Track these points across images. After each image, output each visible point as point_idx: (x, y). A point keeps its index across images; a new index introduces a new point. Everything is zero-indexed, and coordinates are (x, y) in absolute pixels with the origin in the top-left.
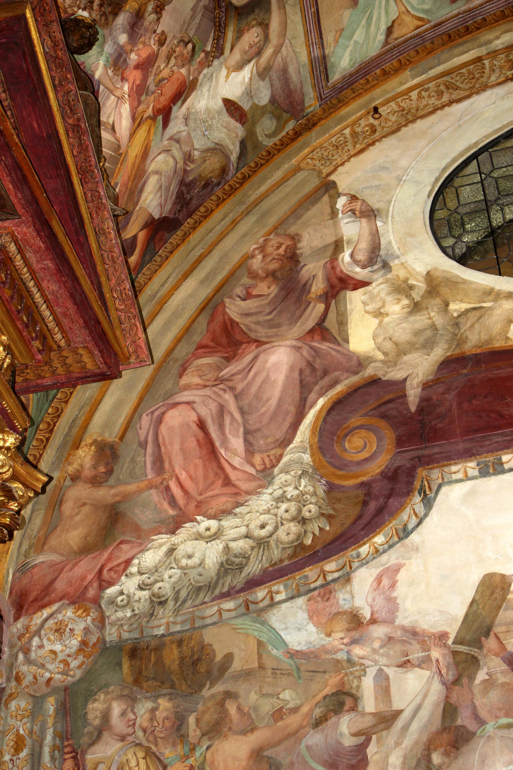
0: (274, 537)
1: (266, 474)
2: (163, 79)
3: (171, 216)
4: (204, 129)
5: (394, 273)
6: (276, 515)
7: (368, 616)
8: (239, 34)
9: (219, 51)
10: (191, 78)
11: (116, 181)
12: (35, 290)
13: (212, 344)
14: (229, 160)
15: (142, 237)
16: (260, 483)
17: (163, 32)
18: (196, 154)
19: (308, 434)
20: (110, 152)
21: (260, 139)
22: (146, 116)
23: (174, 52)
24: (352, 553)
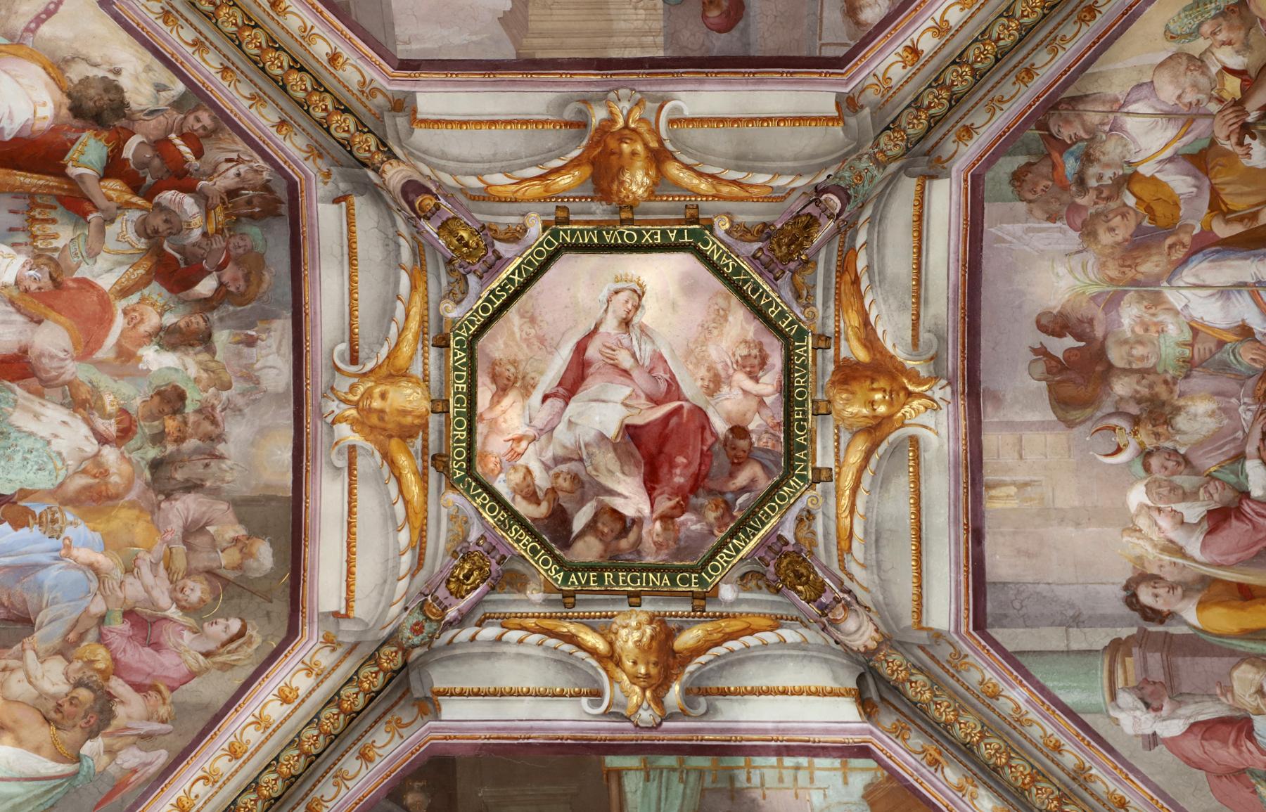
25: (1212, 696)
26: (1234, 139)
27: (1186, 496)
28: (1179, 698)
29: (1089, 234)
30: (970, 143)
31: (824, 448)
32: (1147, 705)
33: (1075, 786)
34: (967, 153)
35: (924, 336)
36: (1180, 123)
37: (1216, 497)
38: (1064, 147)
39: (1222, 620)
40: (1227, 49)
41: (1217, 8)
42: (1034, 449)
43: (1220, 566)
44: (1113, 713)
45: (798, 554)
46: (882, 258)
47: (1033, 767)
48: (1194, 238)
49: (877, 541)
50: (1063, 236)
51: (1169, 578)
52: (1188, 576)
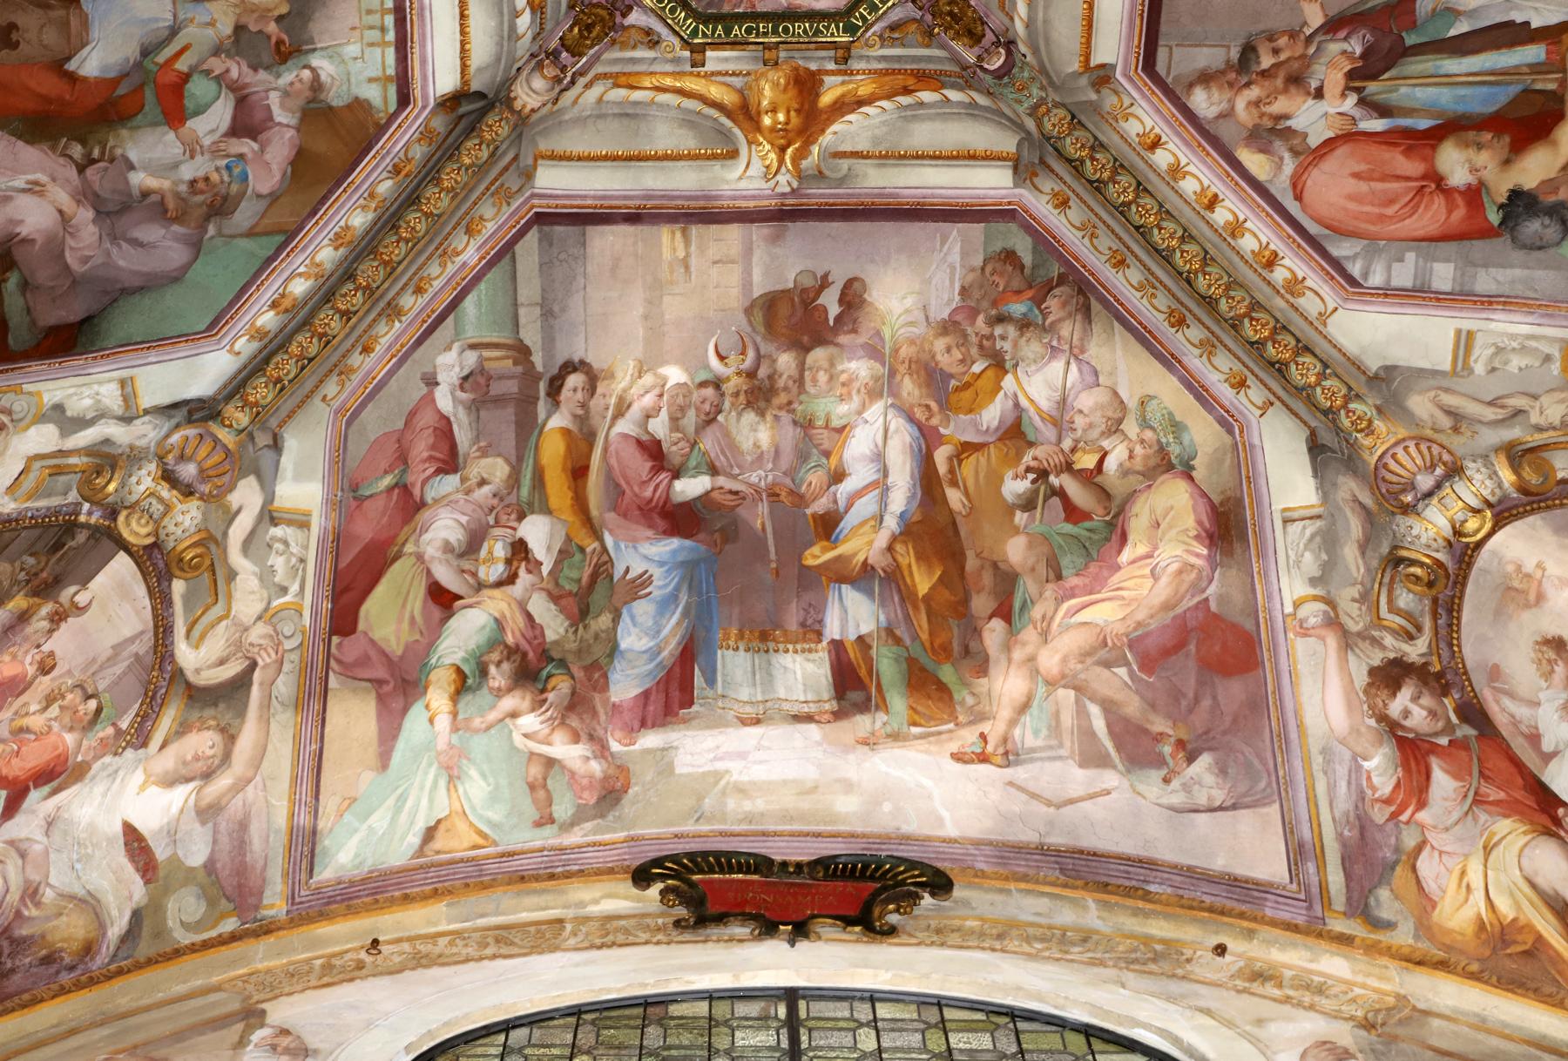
2: (28, 730)
8: (182, 729)
9: (139, 737)
10: (80, 758)
17: (51, 654)
23: (63, 697)
25: (477, 439)
26: (1033, 464)
27: (675, 421)
29: (945, 328)
30: (1050, 207)
31: (726, 60)
33: (382, 304)
34: (1039, 205)
35: (845, 164)
36: (1054, 413)
37: (674, 448)
38: (1039, 301)
39: (552, 450)
40: (1126, 455)
41: (1168, 444)
42: (721, 277)
45: (613, 28)
46: (930, 118)
48: (936, 429)
49: (627, 115)
50: (944, 301)
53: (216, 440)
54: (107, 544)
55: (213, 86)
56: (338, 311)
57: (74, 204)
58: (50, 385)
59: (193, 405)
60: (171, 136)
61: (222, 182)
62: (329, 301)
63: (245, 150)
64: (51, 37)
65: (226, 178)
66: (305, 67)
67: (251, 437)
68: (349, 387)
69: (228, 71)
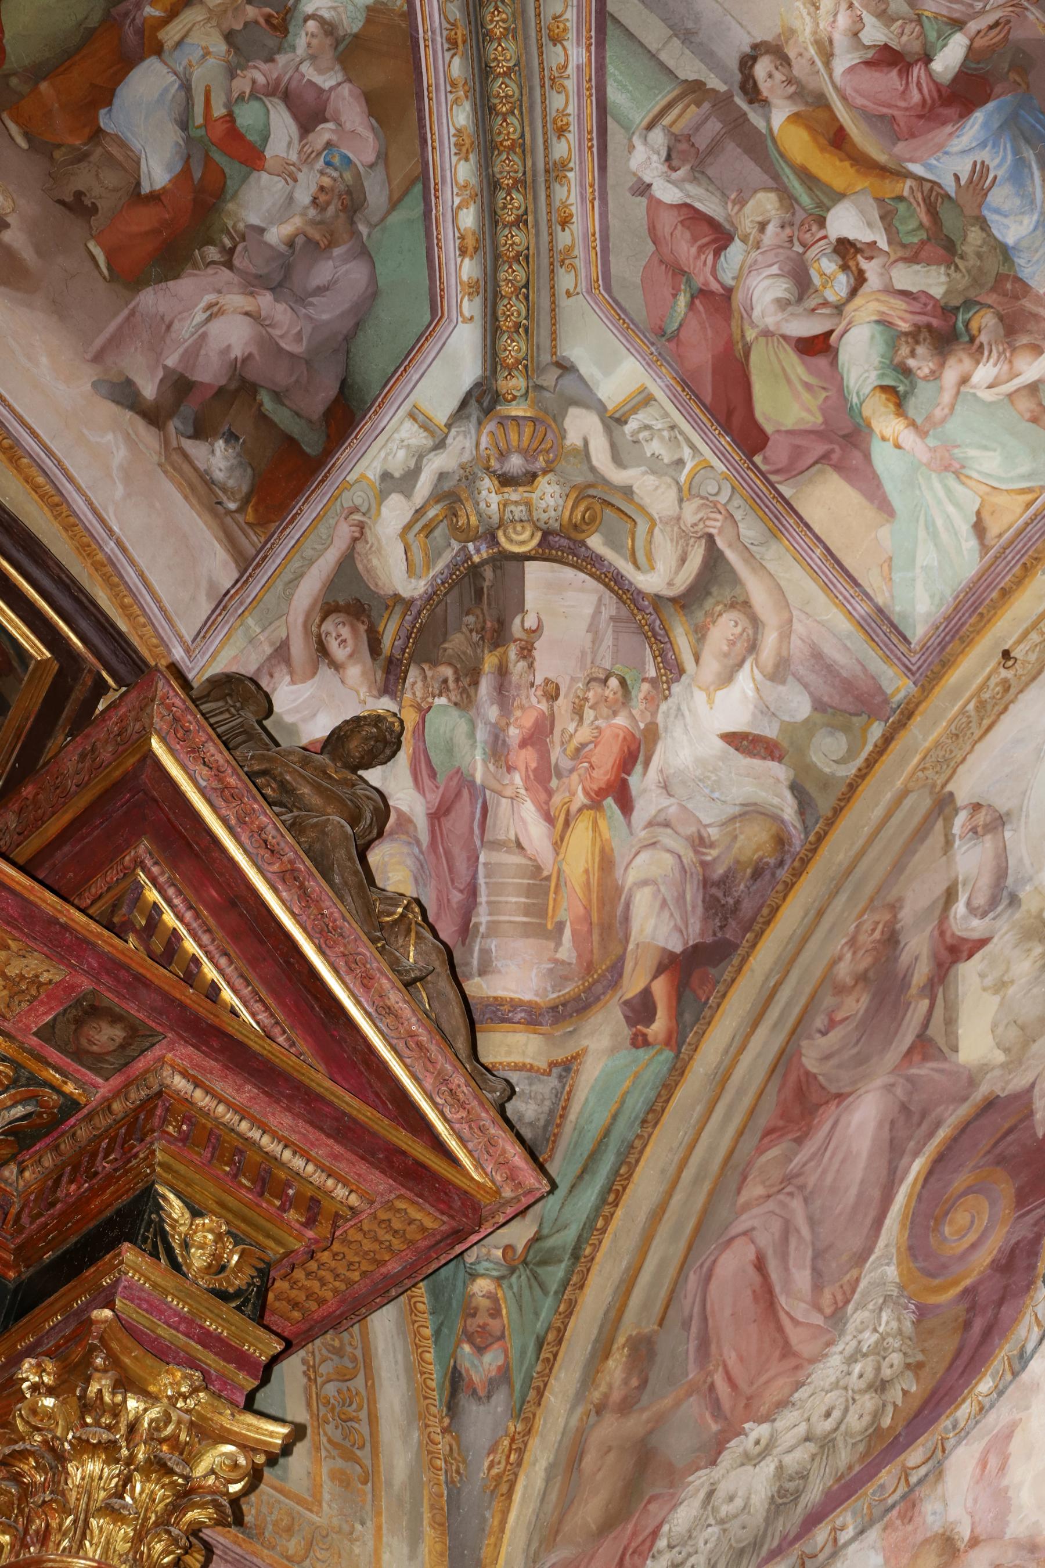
0: (843, 1427)
1: (837, 1317)
2: (584, 745)
3: (709, 940)
4: (707, 791)
5: (1024, 907)
6: (846, 1388)
7: (966, 1534)
10: (642, 726)
11: (557, 919)
12: (255, 1134)
13: (781, 1123)
14: (783, 821)
15: (660, 989)
16: (827, 1337)
17: (547, 681)
18: (713, 833)
19: (896, 1227)
20: (526, 881)
21: (827, 770)
22: (574, 808)
23: (586, 699)
24: (945, 1423)
28: (699, 172)
32: (669, 158)
33: (541, 179)
43: (844, 98)
44: (636, 141)
47: (522, 136)
51: (796, 72)
52: (812, 84)
53: (515, 419)
54: (511, 566)
55: (255, 105)
56: (511, 225)
57: (250, 299)
58: (364, 462)
59: (475, 394)
60: (264, 176)
61: (335, 180)
62: (497, 223)
63: (326, 137)
64: (111, 178)
65: (335, 174)
66: (305, 21)
67: (539, 388)
68: (580, 264)
69: (254, 82)
